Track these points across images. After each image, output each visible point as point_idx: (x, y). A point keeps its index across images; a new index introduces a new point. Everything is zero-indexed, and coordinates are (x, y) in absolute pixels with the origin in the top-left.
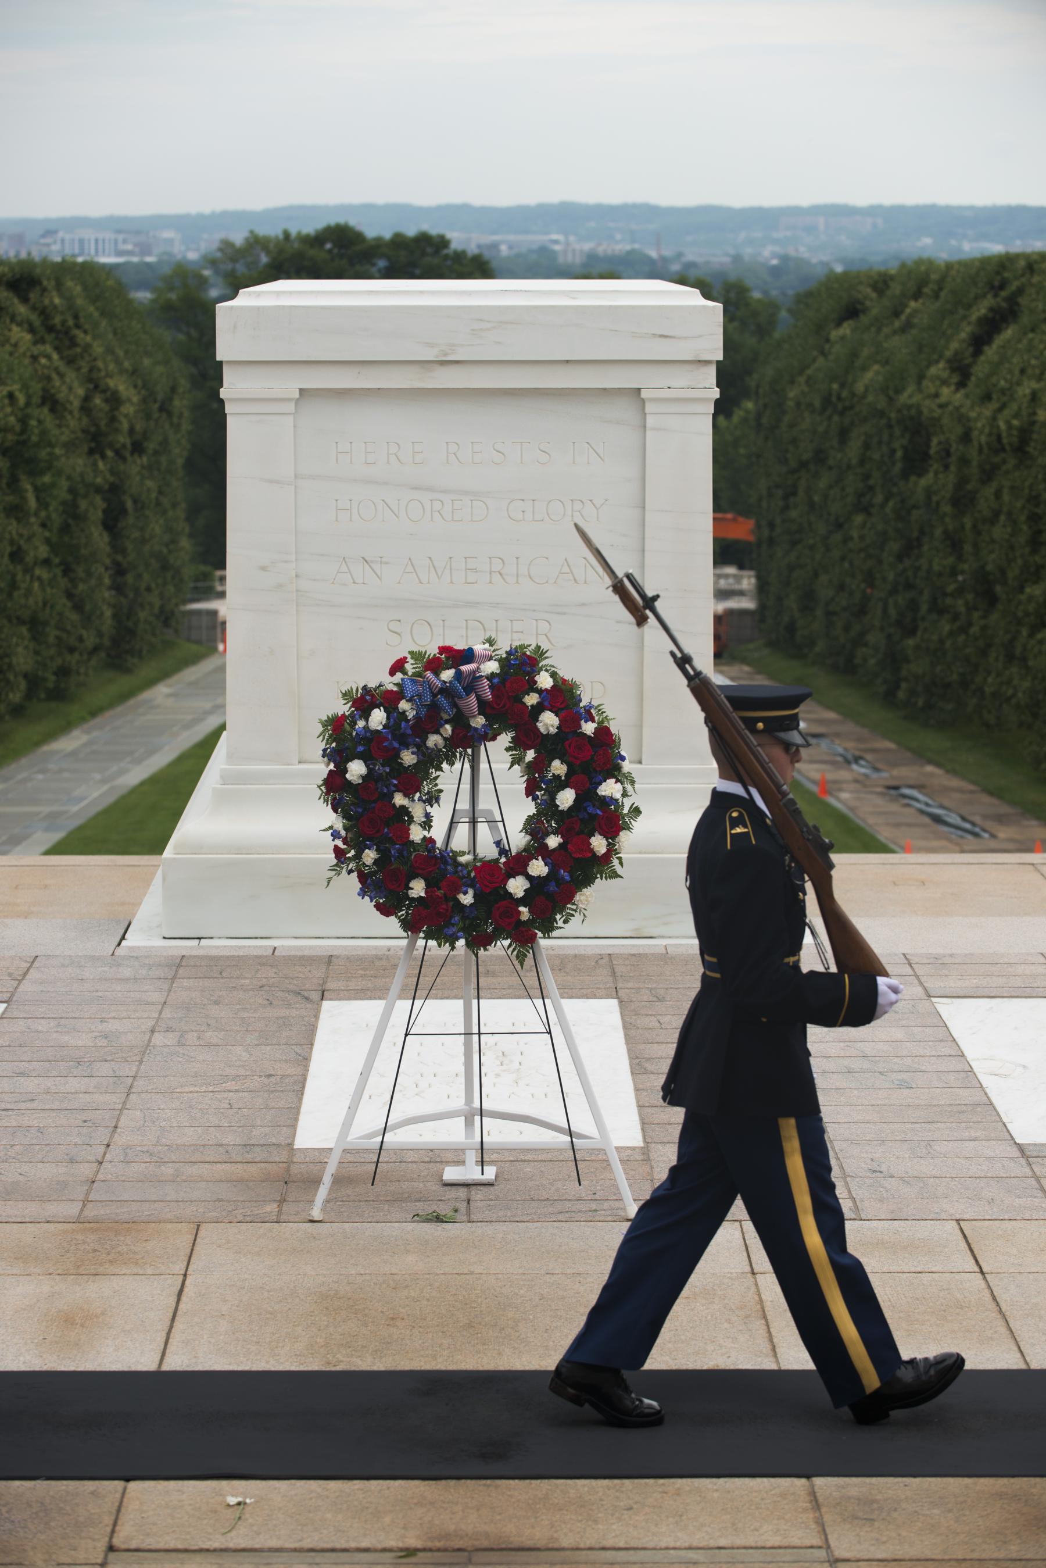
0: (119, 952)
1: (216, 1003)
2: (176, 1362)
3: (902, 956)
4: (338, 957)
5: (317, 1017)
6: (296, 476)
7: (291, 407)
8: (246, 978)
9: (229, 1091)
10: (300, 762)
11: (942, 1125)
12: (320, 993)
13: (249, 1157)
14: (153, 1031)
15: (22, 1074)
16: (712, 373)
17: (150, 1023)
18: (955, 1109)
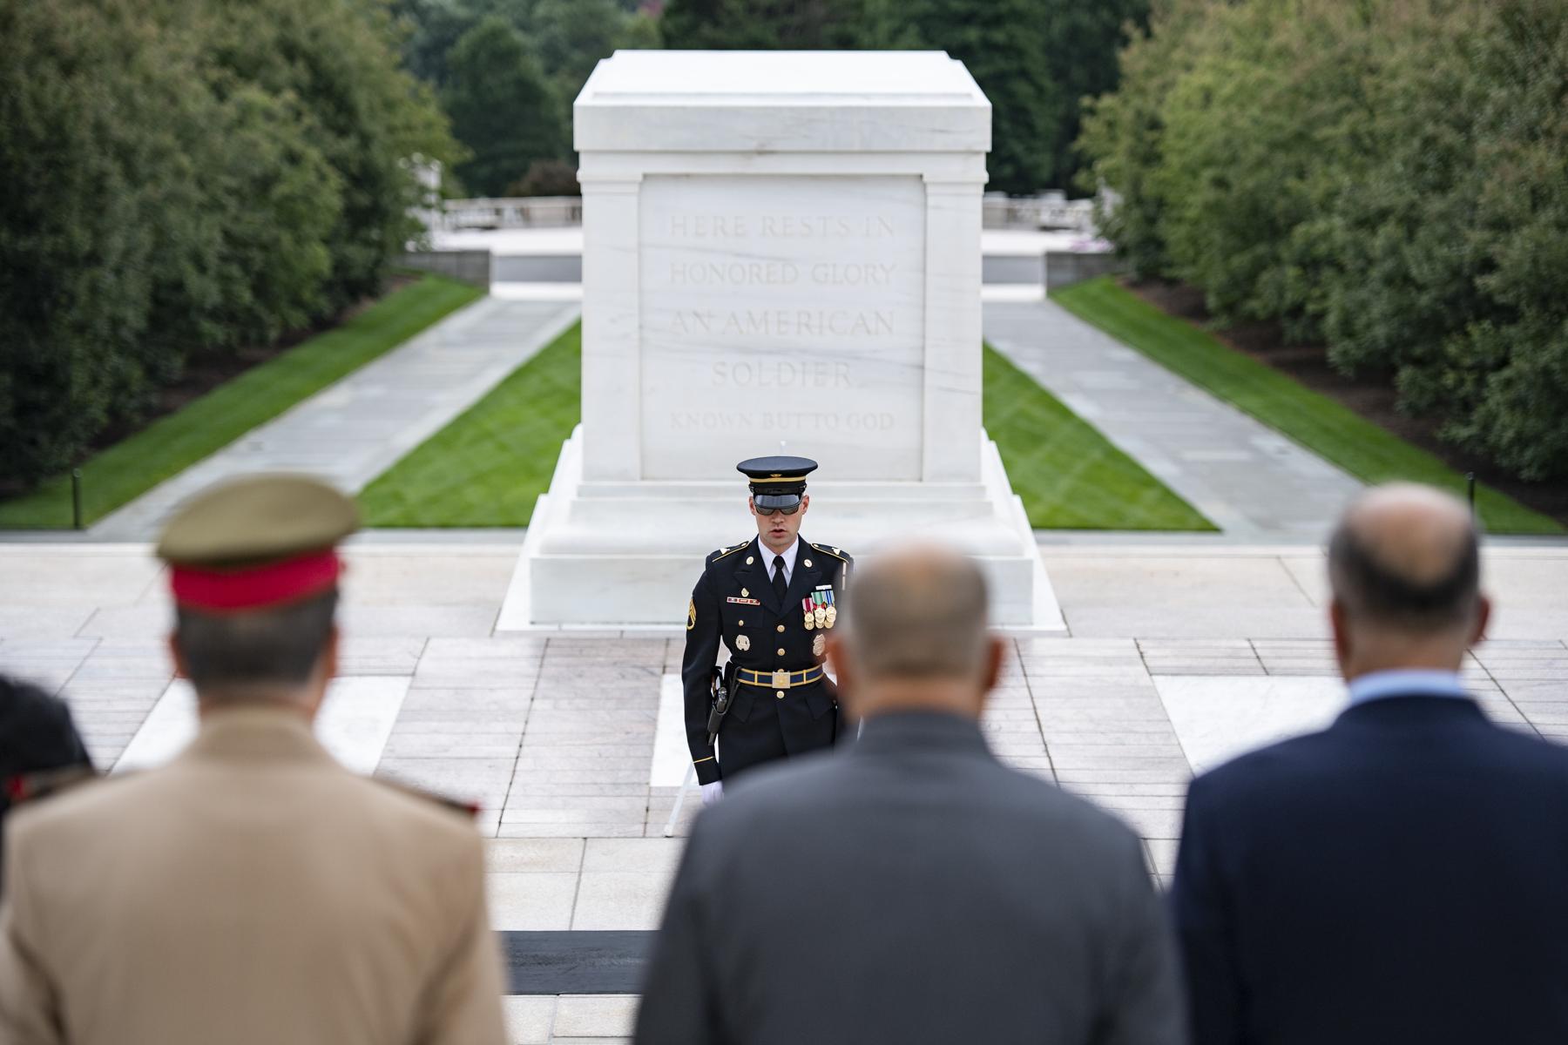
0: (496, 634)
1: (580, 676)
2: (581, 925)
3: (1132, 642)
4: (674, 639)
5: (659, 686)
6: (640, 245)
7: (635, 188)
8: (599, 656)
9: (598, 744)
10: (643, 478)
11: (1141, 772)
12: (661, 670)
13: (617, 792)
14: (532, 699)
15: (436, 732)
16: (982, 160)
17: (530, 693)
18: (1157, 760)
